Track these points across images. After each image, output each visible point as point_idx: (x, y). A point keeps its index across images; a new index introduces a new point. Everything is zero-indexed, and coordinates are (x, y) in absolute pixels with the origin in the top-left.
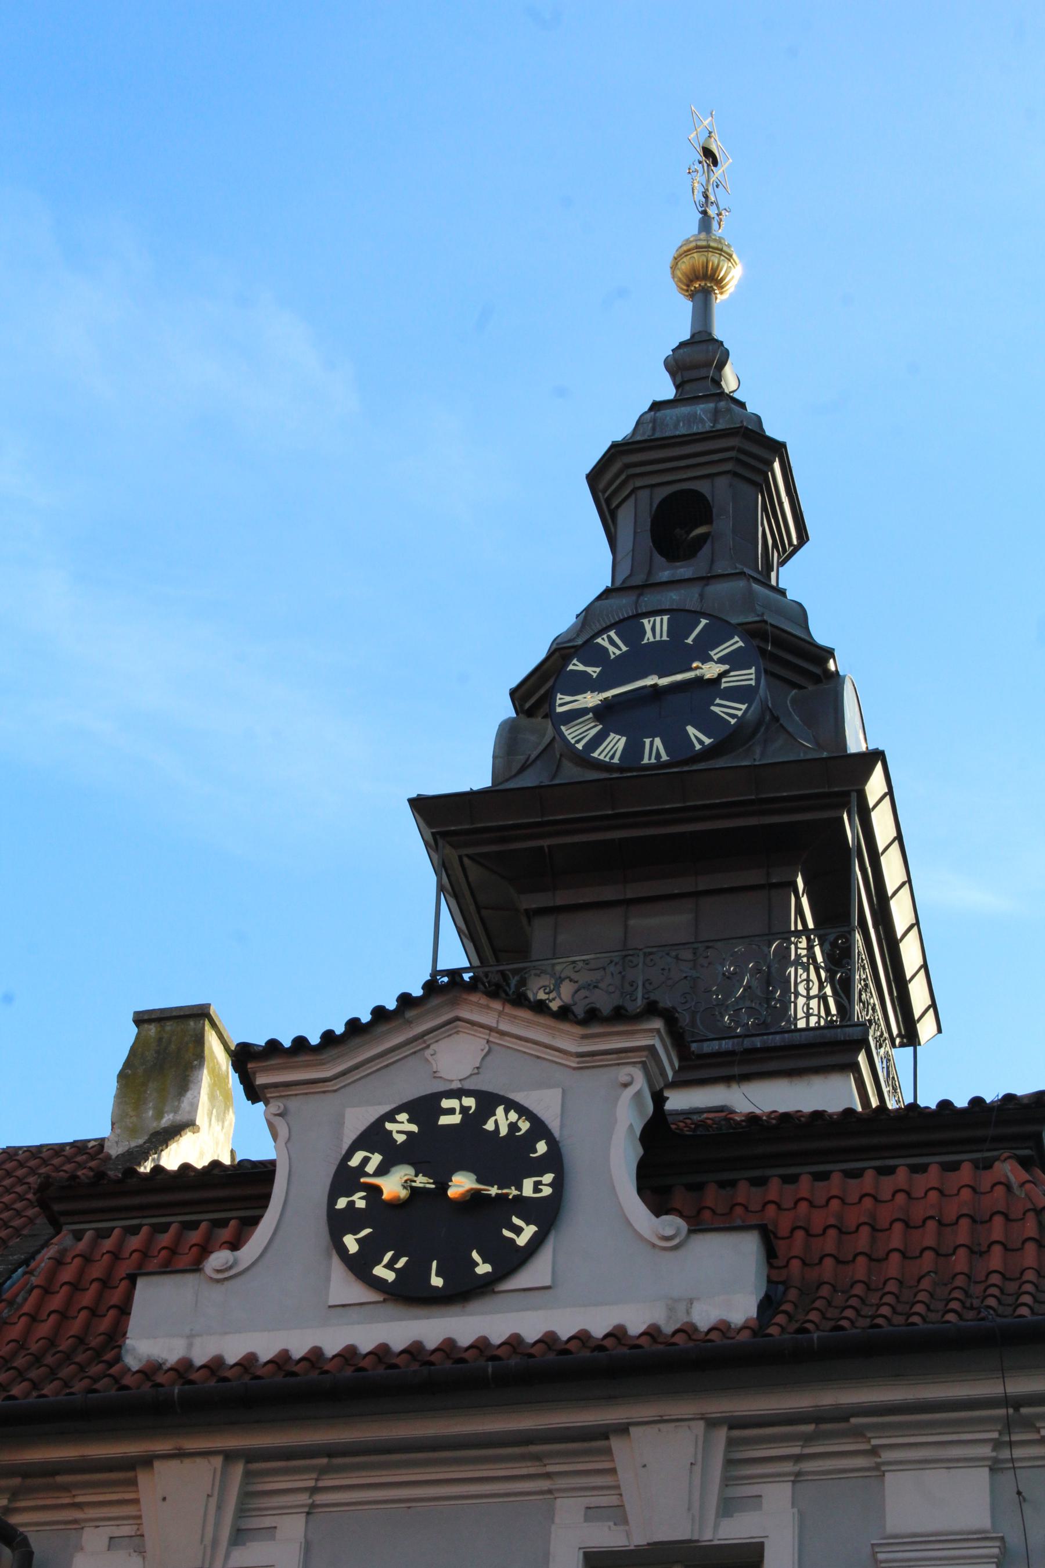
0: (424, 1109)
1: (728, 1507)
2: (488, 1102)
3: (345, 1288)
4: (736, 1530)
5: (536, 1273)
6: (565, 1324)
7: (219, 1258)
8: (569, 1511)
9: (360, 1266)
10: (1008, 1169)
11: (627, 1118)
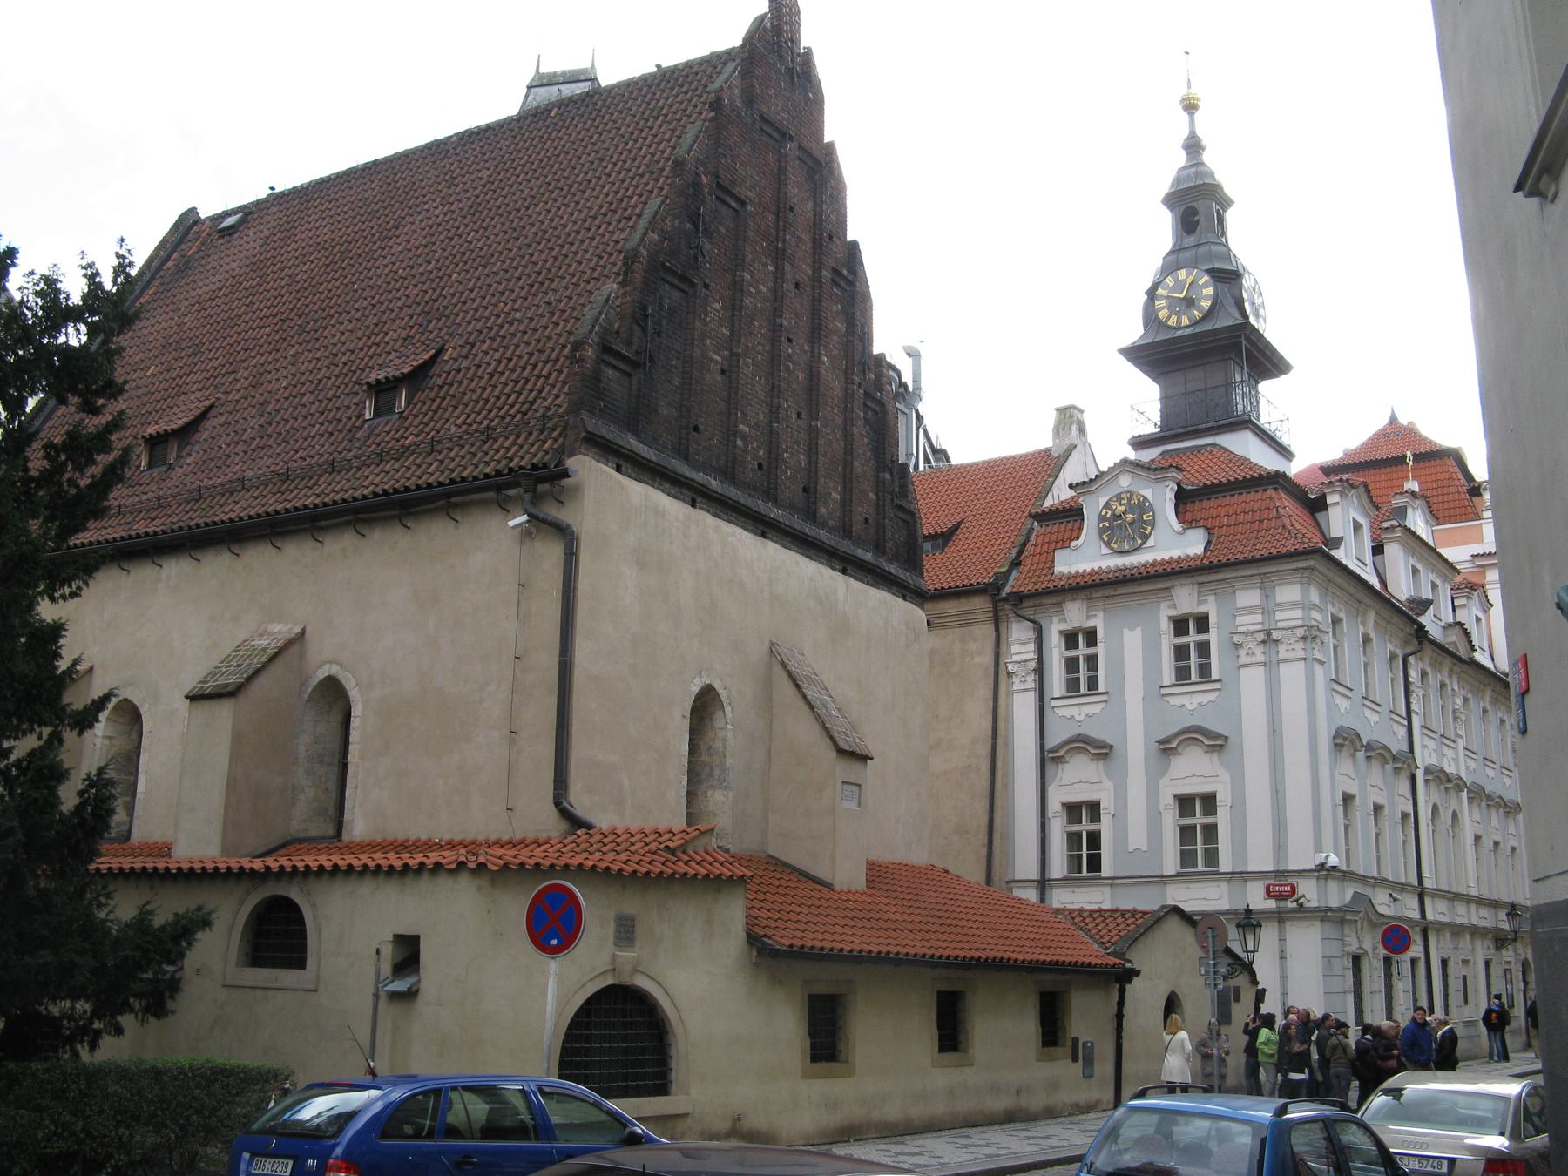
0: (1119, 498)
1: (1200, 603)
2: (1131, 493)
3: (1105, 550)
4: (1202, 609)
5: (1150, 542)
6: (1159, 555)
7: (1073, 544)
8: (1164, 605)
9: (1108, 544)
10: (1270, 492)
11: (1170, 496)
